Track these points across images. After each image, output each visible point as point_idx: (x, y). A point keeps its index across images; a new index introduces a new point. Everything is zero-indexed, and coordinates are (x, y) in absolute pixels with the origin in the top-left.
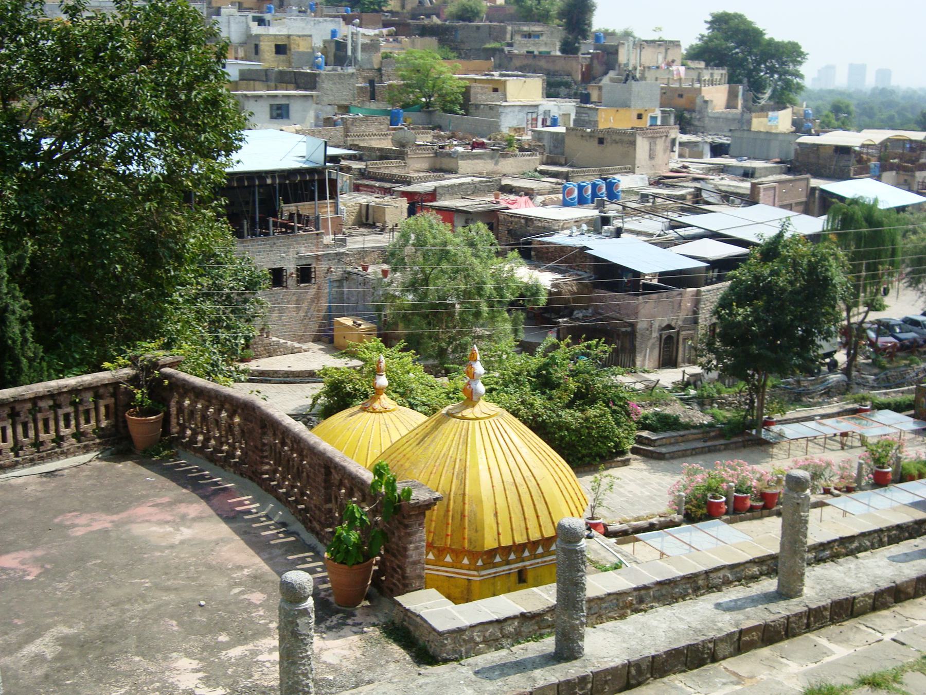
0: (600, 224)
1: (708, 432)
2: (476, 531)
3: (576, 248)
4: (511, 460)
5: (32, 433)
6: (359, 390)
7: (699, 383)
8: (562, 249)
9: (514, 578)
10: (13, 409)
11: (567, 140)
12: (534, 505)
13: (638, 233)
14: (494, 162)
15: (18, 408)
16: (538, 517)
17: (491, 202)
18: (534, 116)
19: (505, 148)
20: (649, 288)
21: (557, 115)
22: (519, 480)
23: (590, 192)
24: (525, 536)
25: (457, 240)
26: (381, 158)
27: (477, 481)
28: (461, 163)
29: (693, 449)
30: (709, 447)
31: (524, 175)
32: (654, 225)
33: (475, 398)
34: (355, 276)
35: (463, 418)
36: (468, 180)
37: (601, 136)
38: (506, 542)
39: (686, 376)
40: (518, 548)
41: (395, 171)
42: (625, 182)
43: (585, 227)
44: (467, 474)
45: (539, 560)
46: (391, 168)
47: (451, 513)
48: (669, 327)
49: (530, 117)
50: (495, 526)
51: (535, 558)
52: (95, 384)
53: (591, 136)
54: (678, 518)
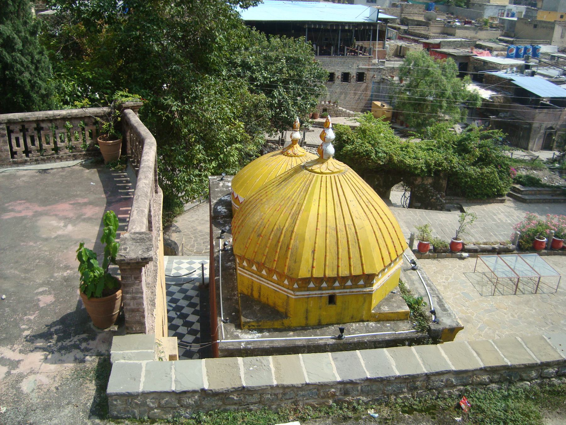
0: (522, 70)
1: (555, 191)
2: (295, 262)
3: (507, 79)
4: (338, 210)
5: (37, 143)
6: (350, 139)
7: (562, 161)
8: (499, 79)
9: (325, 300)
10: (23, 126)
11: (517, 25)
12: (349, 248)
13: (544, 76)
14: (475, 32)
15: (26, 126)
16: (350, 258)
17: (468, 52)
18: (503, 11)
19: (483, 26)
20: (544, 106)
21: (515, 12)
22: (341, 226)
23: (522, 51)
24: (335, 272)
25: (435, 66)
26: (417, 25)
27: (305, 223)
28: (457, 31)
29: (544, 199)
30: (554, 199)
31: (490, 40)
32: (554, 72)
33: (324, 157)
34: (386, 81)
35: (312, 171)
36: (459, 40)
37: (536, 23)
38: (318, 273)
39: (555, 156)
40: (332, 280)
41: (423, 32)
42: (544, 49)
43: (515, 69)
44: (300, 216)
45: (348, 290)
46: (421, 30)
47: (280, 244)
48: (551, 128)
49: (500, 11)
50: (311, 260)
51: (344, 288)
52: (80, 116)
53: (530, 23)
54: (511, 246)
